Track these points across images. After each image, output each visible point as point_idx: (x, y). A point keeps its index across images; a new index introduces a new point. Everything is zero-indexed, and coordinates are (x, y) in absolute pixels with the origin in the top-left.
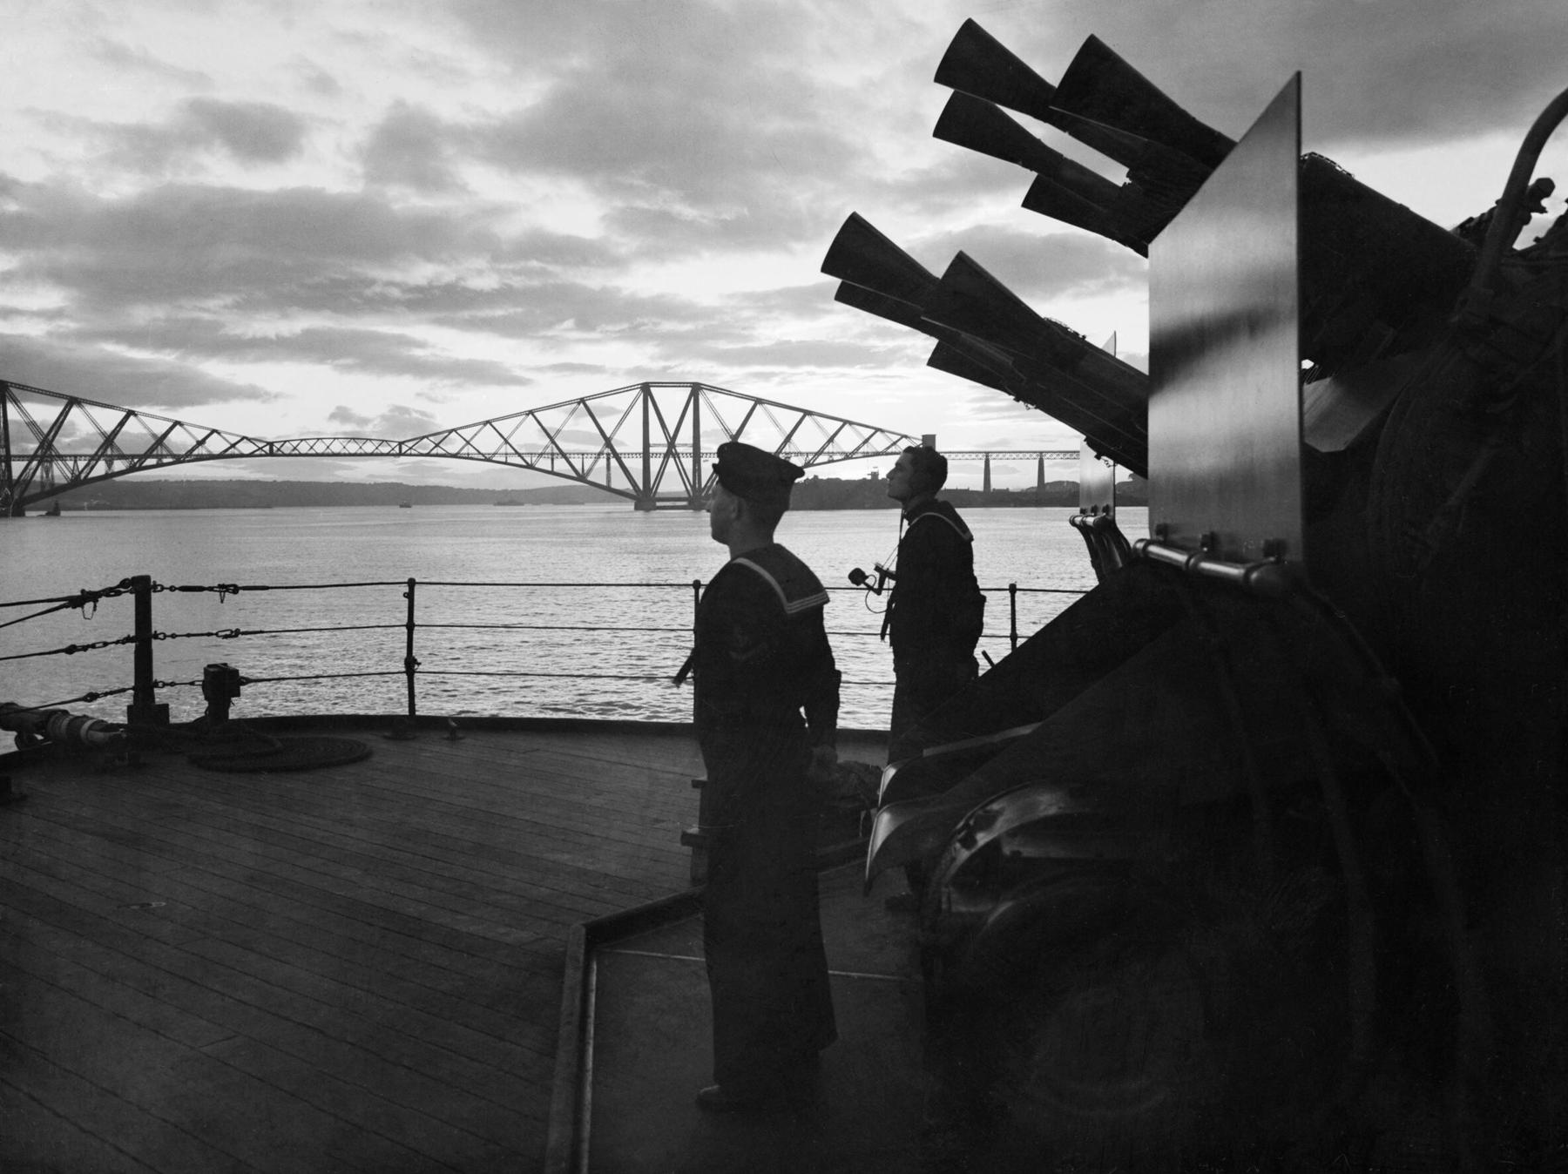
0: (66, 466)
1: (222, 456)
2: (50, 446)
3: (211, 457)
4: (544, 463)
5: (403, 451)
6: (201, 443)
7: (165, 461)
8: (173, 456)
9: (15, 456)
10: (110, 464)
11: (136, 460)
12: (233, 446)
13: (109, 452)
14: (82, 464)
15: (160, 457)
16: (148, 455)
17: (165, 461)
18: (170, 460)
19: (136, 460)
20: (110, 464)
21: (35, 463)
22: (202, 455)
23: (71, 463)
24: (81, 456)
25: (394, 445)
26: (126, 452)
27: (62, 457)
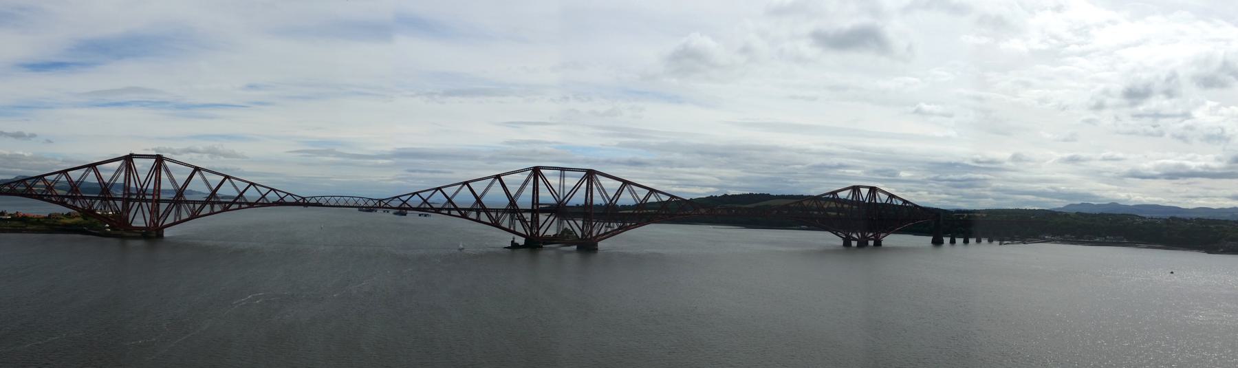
0: (189, 207)
3: (269, 204)
4: (473, 215)
5: (382, 205)
8: (248, 203)
10: (212, 208)
11: (227, 205)
14: (197, 206)
15: (240, 203)
16: (234, 202)
17: (243, 206)
18: (246, 206)
19: (227, 205)
20: (212, 208)
23: (191, 205)
24: (197, 201)
25: (376, 202)
27: (187, 202)
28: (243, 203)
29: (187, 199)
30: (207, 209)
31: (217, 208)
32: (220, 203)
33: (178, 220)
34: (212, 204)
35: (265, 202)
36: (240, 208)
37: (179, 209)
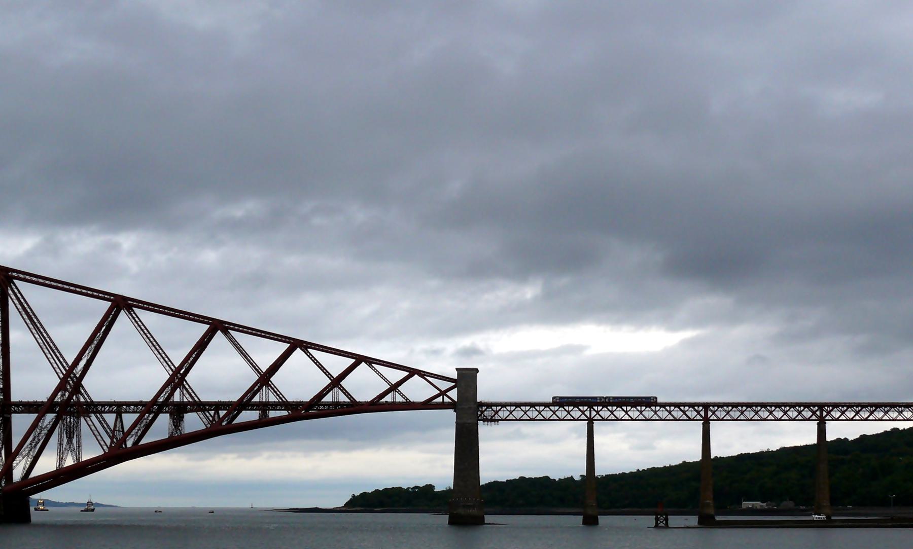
0: (103, 422)
1: (376, 406)
2: (78, 387)
3: (354, 407)
6: (336, 382)
7: (273, 414)
8: (284, 404)
9: (18, 404)
11: (222, 413)
12: (394, 387)
13: (177, 397)
14: (129, 419)
15: (264, 407)
16: (244, 404)
17: (273, 414)
18: (285, 413)
19: (222, 413)
21: (50, 417)
22: (336, 404)
23: (110, 418)
24: (128, 404)
26: (204, 398)
28: (274, 406)
29: (96, 399)
30: (162, 426)
31: (193, 422)
32: (200, 406)
33: (69, 461)
34: (178, 411)
35: (343, 398)
36: (264, 422)
37: (71, 433)
